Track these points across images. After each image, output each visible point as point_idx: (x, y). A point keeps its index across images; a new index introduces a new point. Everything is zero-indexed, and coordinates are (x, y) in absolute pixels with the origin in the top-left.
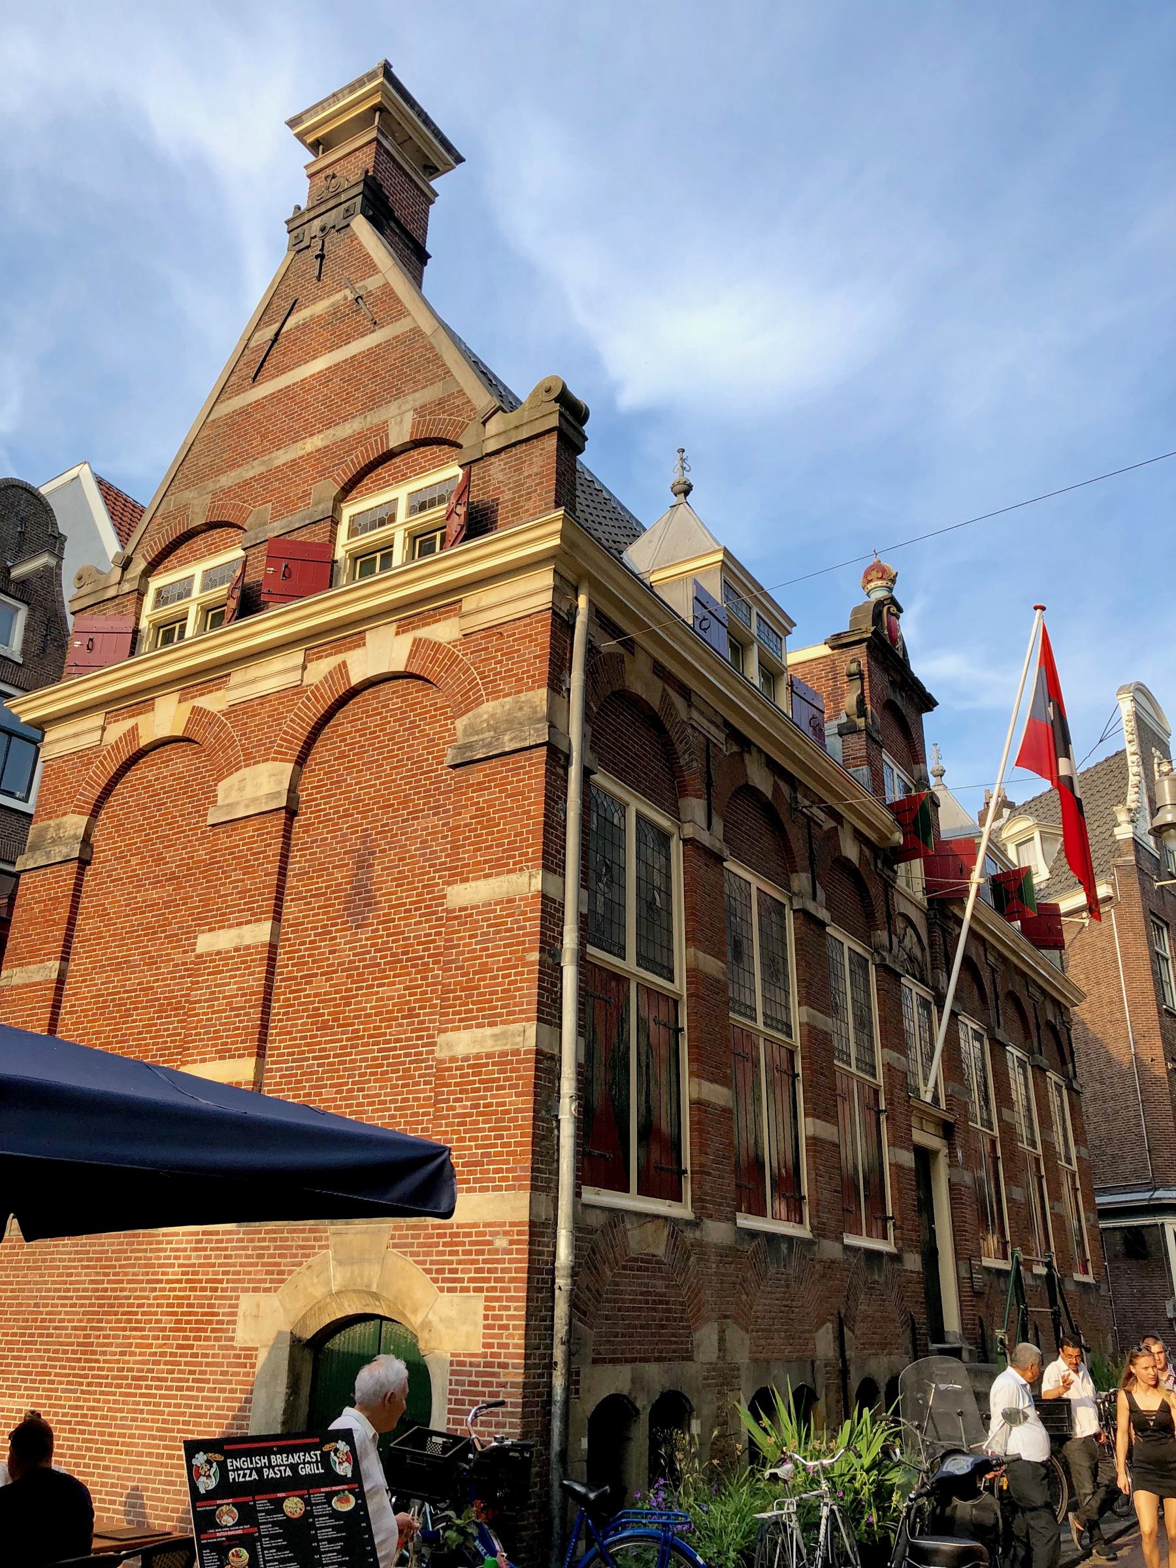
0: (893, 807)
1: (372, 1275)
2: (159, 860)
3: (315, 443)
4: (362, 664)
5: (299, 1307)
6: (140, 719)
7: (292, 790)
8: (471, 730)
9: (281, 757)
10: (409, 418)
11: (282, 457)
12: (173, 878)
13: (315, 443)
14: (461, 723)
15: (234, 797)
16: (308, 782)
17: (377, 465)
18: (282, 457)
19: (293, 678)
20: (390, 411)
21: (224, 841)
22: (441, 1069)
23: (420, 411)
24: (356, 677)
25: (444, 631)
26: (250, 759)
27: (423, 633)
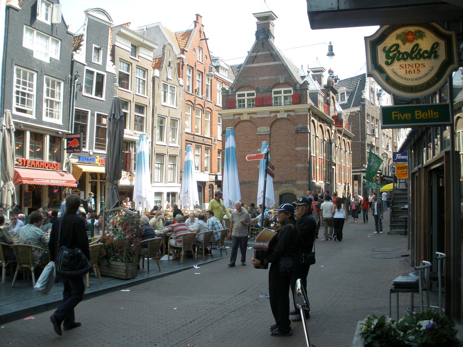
0: (333, 117)
1: (289, 189)
2: (247, 137)
3: (266, 78)
4: (279, 116)
5: (280, 192)
6: (240, 116)
7: (270, 131)
8: (297, 128)
9: (267, 126)
10: (283, 79)
11: (261, 78)
12: (250, 140)
13: (266, 78)
14: (296, 127)
15: (260, 131)
16: (272, 131)
17: (278, 85)
18: (261, 78)
19: (268, 115)
20: (280, 77)
21: (259, 137)
22: (296, 169)
23: (285, 78)
24: (279, 117)
25: (292, 114)
26: (262, 126)
27: (289, 113)
